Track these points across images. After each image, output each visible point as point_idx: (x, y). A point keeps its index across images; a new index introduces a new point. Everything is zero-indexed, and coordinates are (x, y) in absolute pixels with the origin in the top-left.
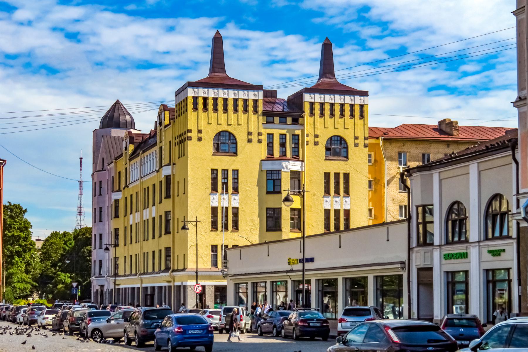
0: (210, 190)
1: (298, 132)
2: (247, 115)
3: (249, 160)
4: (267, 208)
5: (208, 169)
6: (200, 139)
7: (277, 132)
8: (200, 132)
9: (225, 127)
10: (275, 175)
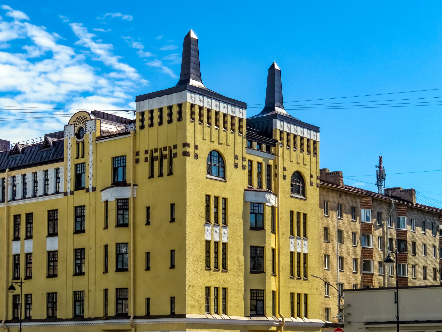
0: (204, 221)
1: (271, 162)
2: (234, 134)
3: (235, 187)
4: (251, 247)
5: (203, 194)
6: (196, 156)
7: (256, 159)
8: (196, 147)
9: (216, 146)
10: (257, 208)
